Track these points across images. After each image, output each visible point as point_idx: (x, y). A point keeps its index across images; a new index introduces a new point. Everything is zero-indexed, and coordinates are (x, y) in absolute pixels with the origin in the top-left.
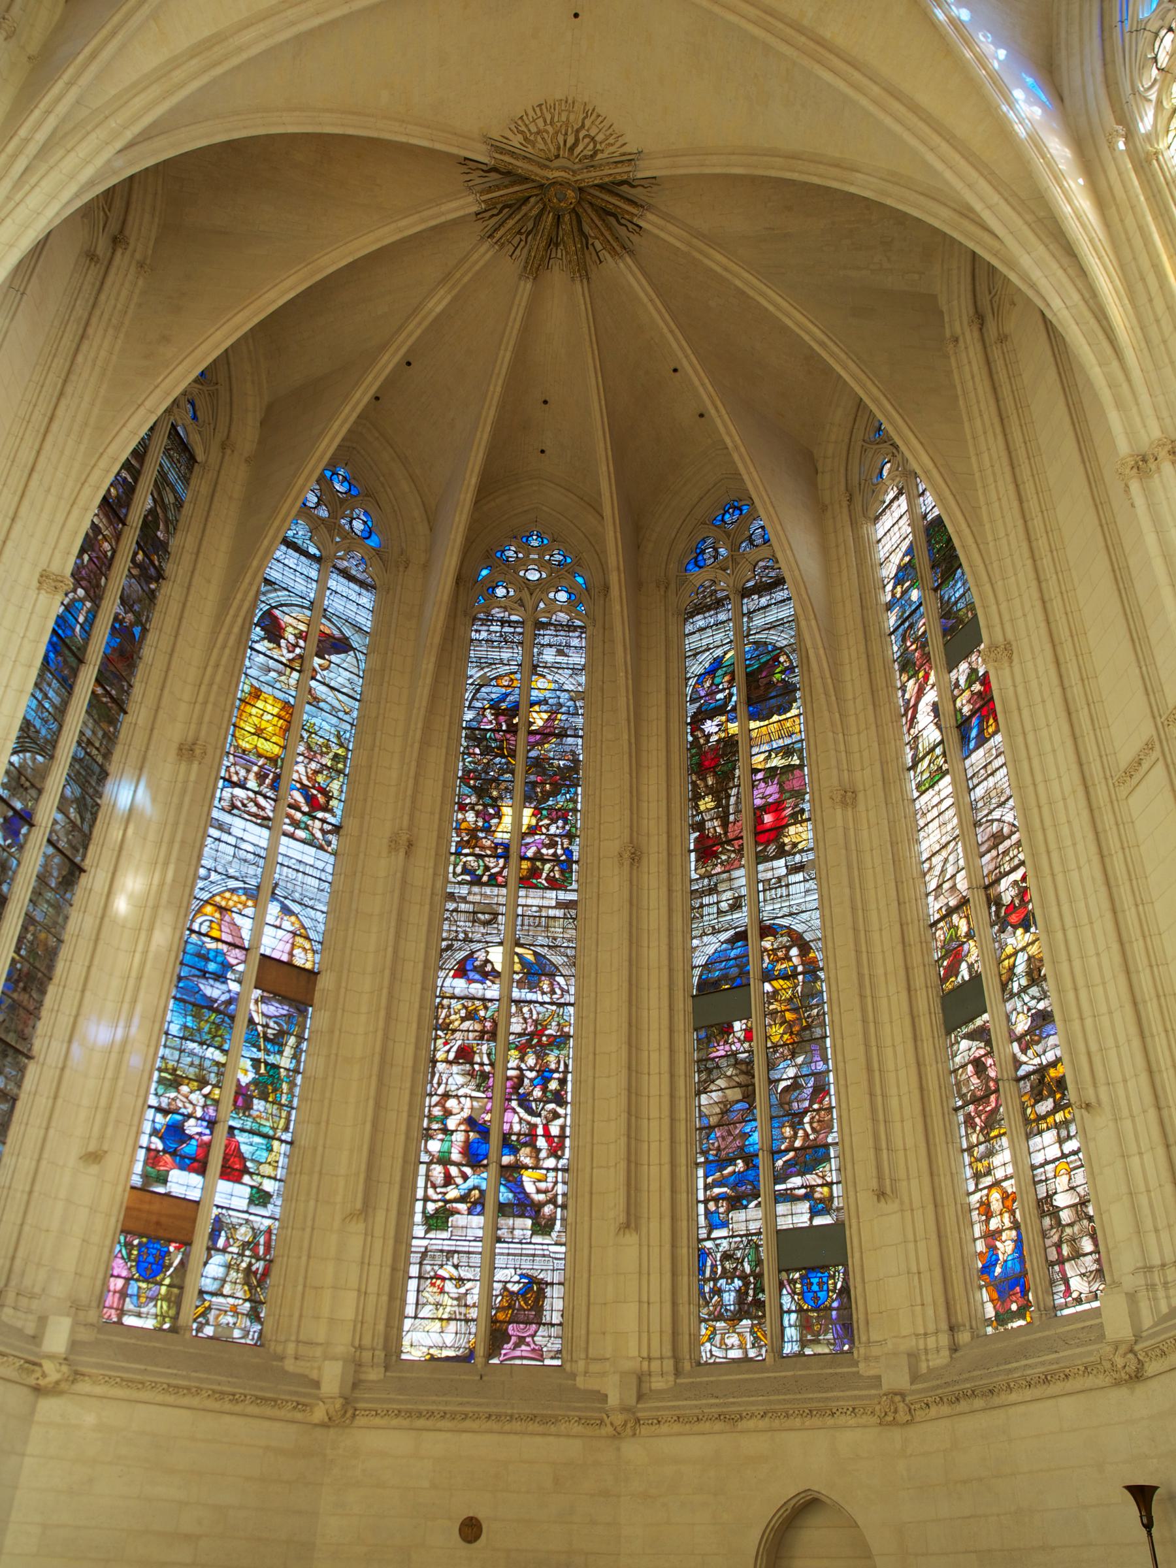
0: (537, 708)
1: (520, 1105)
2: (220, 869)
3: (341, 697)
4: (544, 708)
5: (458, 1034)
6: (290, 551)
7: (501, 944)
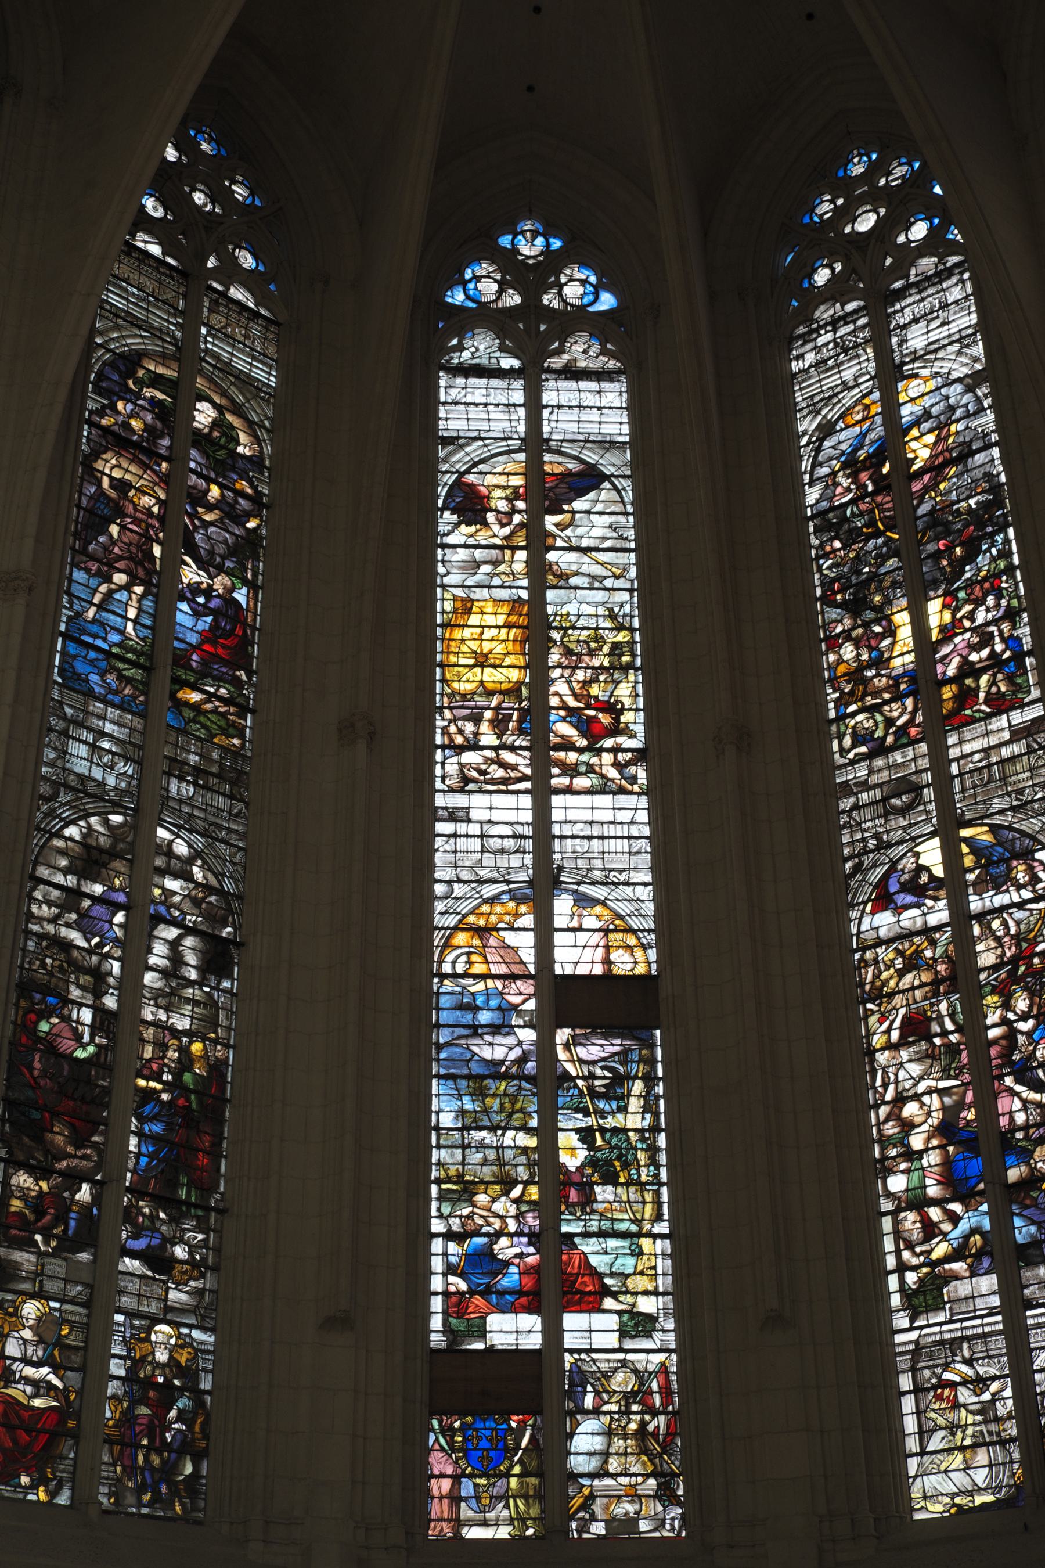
0: (915, 432)
1: (1018, 1081)
2: (465, 875)
3: (603, 557)
4: (926, 426)
5: (898, 1000)
6: (473, 381)
7: (933, 834)
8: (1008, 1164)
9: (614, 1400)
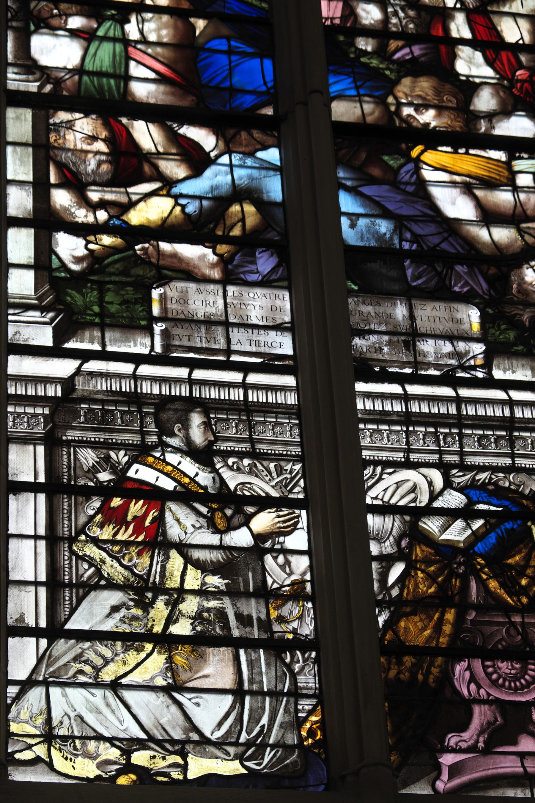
8: (334, 89)
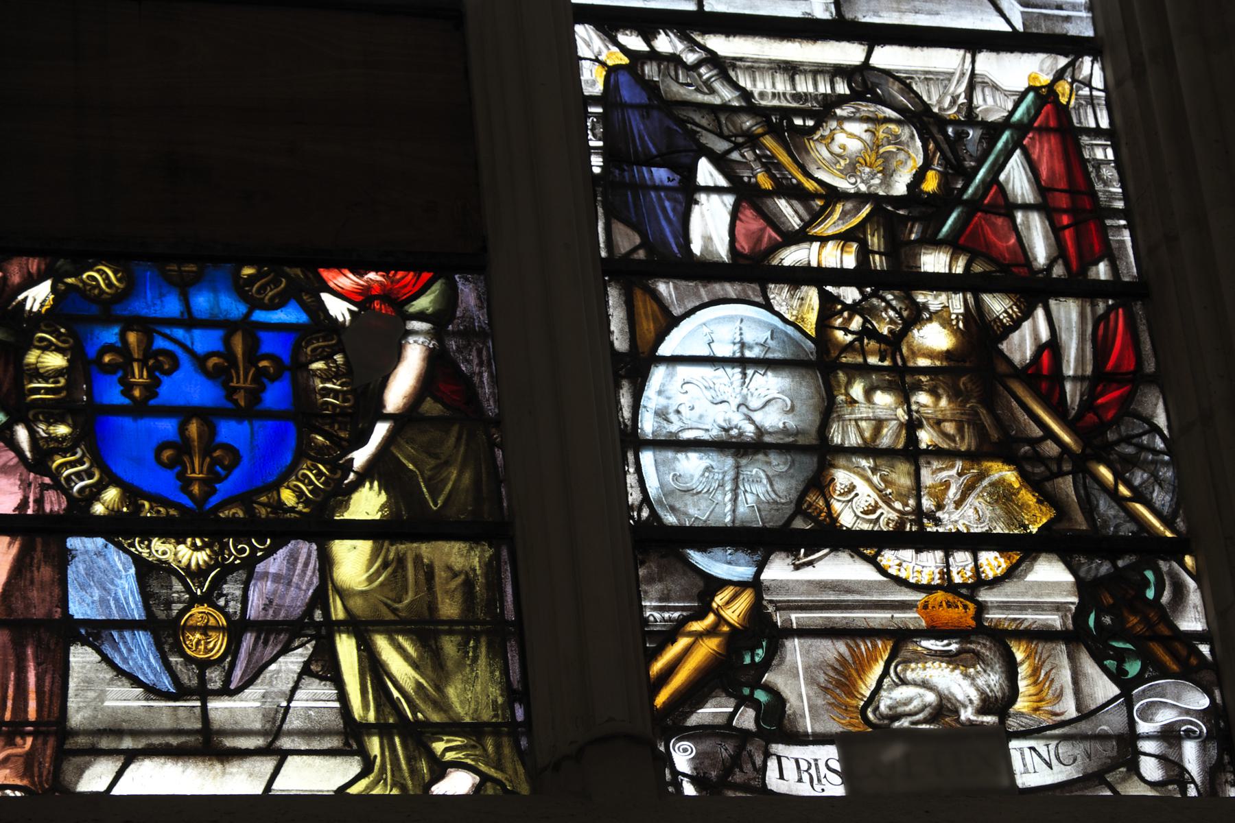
9: (832, 225)
